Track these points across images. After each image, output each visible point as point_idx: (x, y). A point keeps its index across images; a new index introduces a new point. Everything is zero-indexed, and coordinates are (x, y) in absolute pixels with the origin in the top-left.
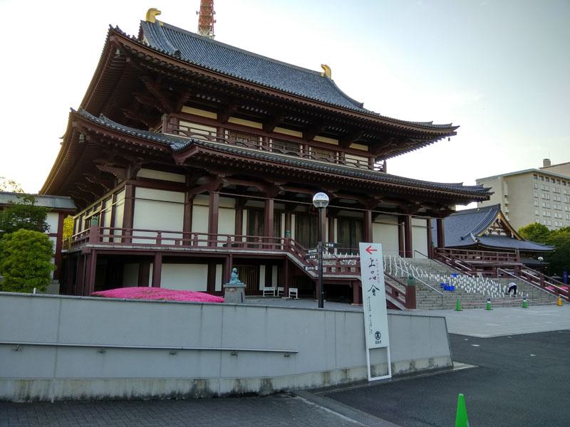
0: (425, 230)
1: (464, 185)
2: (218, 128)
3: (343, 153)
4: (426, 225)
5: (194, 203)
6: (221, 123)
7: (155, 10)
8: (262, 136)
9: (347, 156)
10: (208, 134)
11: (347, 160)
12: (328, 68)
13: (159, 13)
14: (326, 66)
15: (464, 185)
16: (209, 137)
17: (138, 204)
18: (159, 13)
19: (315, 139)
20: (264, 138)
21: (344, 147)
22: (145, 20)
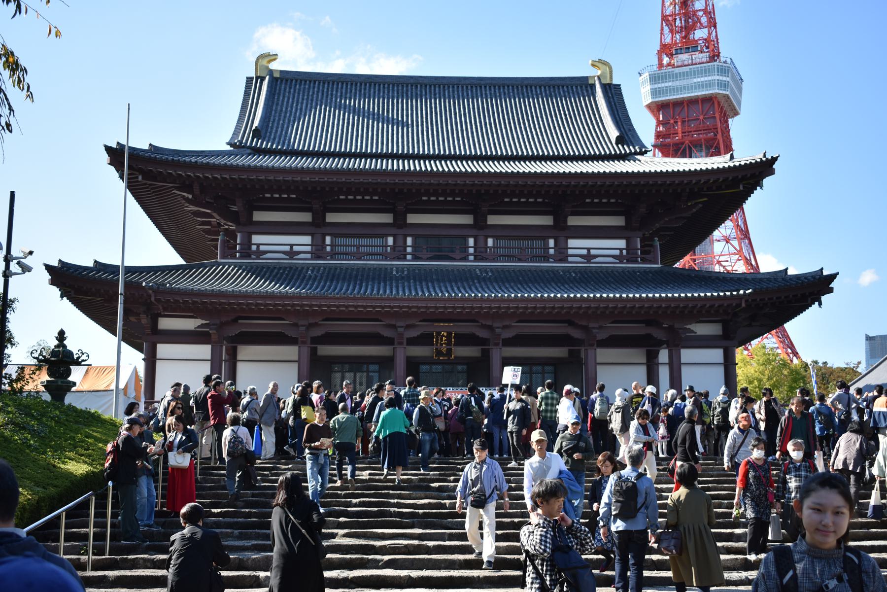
0: (721, 370)
1: (790, 272)
2: (312, 235)
3: (562, 239)
4: (722, 361)
5: (239, 357)
6: (317, 228)
7: (268, 55)
8: (390, 235)
9: (572, 243)
10: (287, 248)
11: (570, 252)
12: (605, 63)
13: (273, 57)
14: (600, 61)
15: (790, 272)
16: (291, 254)
17: (159, 365)
18: (275, 59)
19: (489, 222)
20: (395, 236)
21: (563, 232)
22: (252, 74)
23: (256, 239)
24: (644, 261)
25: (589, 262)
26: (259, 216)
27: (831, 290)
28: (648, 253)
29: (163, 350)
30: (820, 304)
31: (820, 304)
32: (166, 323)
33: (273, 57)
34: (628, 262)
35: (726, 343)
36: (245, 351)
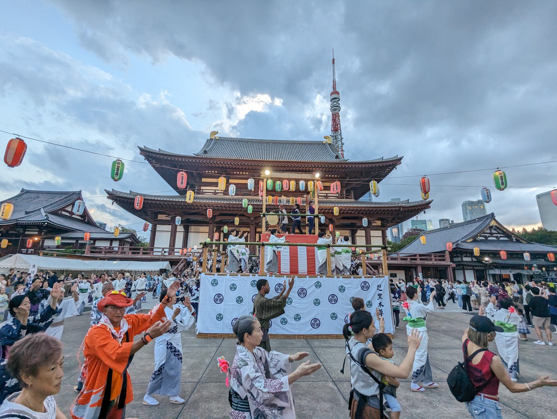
10: (214, 191)
13: (217, 133)
23: (202, 188)
24: (347, 198)
25: (327, 198)
26: (204, 180)
27: (429, 207)
28: (349, 195)
29: (159, 227)
30: (425, 212)
31: (425, 212)
32: (161, 217)
33: (217, 133)
34: (341, 198)
35: (383, 228)
36: (192, 228)
